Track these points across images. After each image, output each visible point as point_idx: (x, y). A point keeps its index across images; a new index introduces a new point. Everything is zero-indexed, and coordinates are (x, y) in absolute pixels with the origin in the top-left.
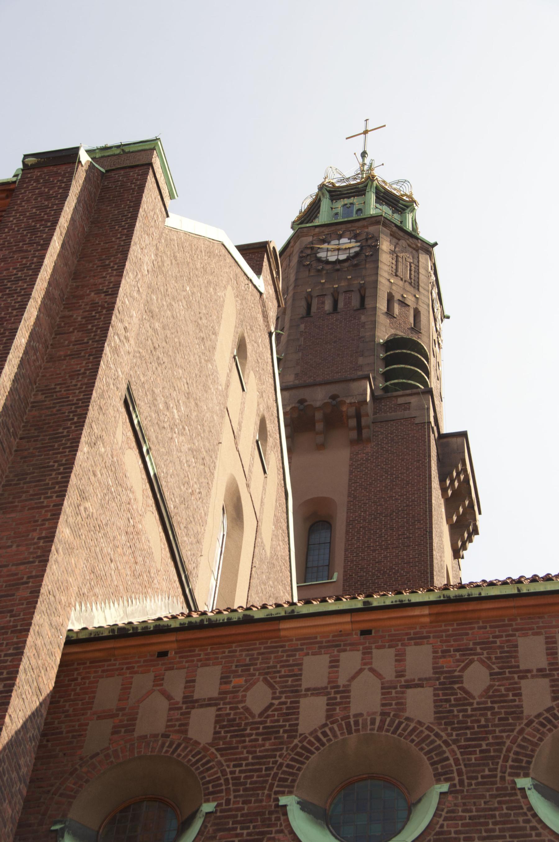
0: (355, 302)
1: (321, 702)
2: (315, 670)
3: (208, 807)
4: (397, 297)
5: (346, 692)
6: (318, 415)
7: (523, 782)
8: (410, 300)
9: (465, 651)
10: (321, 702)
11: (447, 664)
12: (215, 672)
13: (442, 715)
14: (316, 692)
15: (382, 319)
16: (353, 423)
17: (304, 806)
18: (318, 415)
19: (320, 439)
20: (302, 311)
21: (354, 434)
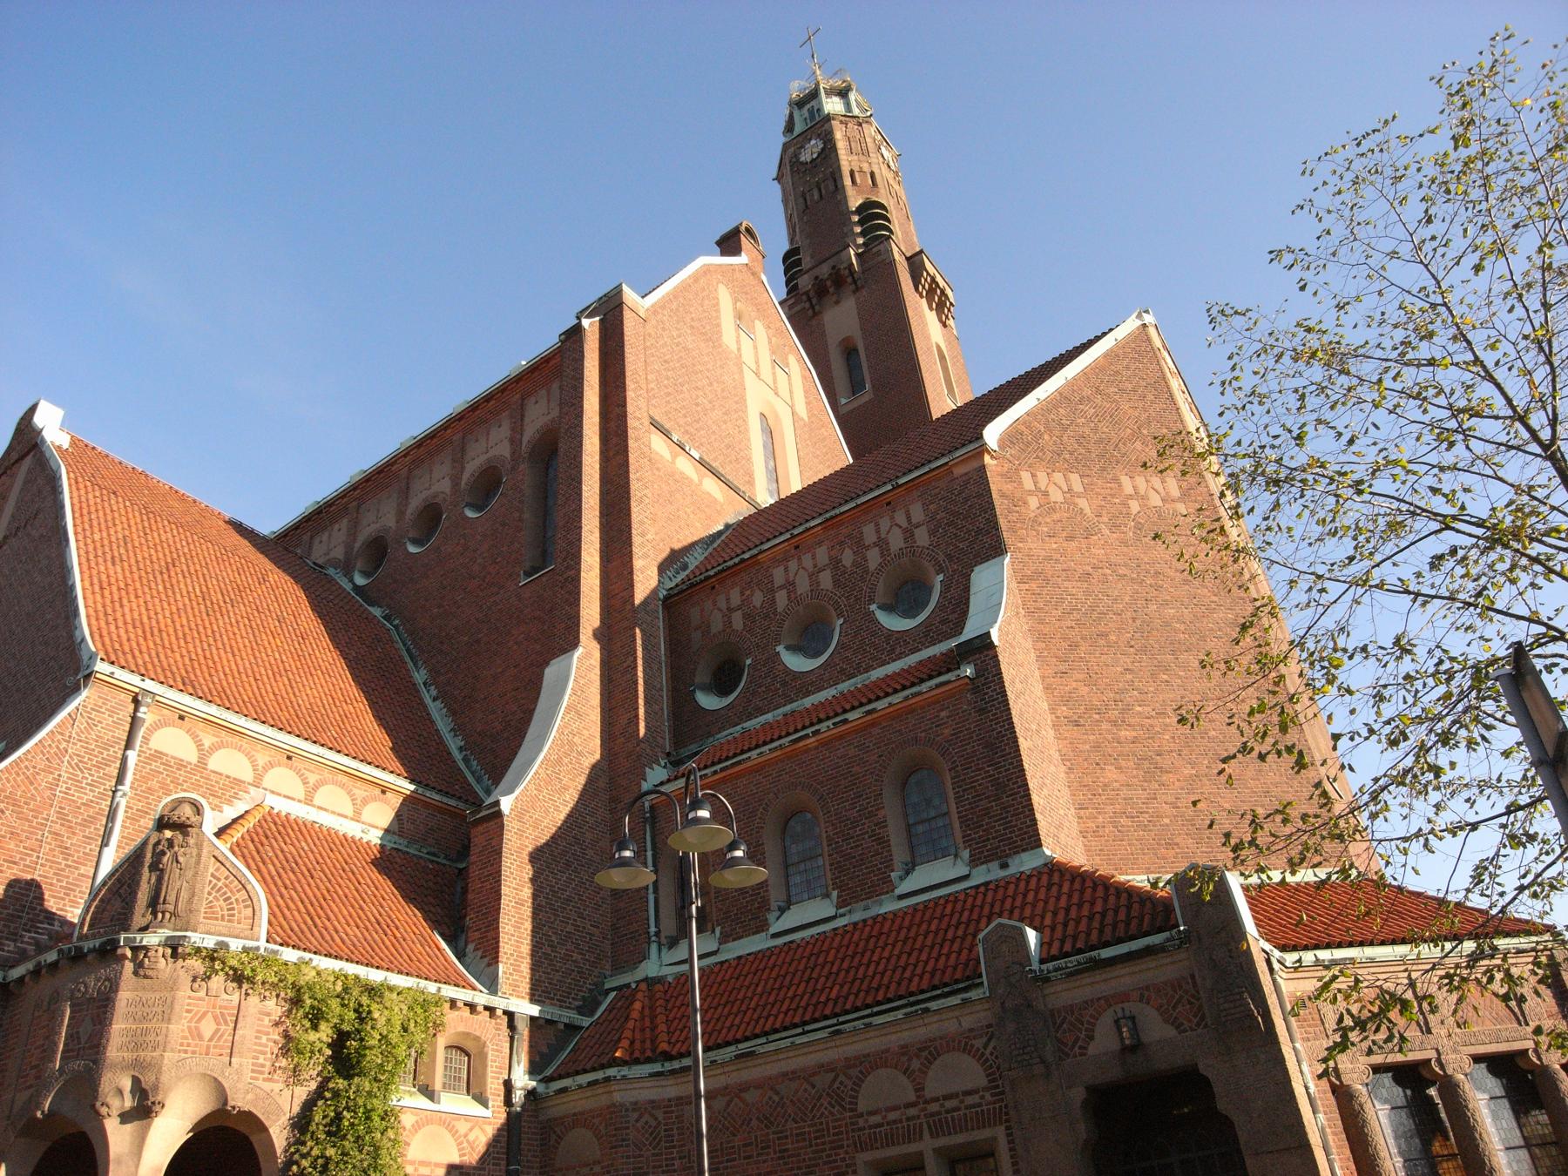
0: (832, 188)
1: (784, 592)
2: (778, 575)
3: (748, 662)
4: (856, 169)
5: (793, 584)
6: (829, 283)
7: (873, 607)
8: (866, 167)
9: (841, 543)
10: (784, 592)
12: (737, 589)
14: (781, 587)
15: (850, 190)
16: (849, 280)
17: (788, 648)
18: (829, 283)
19: (834, 298)
20: (802, 207)
21: (853, 287)
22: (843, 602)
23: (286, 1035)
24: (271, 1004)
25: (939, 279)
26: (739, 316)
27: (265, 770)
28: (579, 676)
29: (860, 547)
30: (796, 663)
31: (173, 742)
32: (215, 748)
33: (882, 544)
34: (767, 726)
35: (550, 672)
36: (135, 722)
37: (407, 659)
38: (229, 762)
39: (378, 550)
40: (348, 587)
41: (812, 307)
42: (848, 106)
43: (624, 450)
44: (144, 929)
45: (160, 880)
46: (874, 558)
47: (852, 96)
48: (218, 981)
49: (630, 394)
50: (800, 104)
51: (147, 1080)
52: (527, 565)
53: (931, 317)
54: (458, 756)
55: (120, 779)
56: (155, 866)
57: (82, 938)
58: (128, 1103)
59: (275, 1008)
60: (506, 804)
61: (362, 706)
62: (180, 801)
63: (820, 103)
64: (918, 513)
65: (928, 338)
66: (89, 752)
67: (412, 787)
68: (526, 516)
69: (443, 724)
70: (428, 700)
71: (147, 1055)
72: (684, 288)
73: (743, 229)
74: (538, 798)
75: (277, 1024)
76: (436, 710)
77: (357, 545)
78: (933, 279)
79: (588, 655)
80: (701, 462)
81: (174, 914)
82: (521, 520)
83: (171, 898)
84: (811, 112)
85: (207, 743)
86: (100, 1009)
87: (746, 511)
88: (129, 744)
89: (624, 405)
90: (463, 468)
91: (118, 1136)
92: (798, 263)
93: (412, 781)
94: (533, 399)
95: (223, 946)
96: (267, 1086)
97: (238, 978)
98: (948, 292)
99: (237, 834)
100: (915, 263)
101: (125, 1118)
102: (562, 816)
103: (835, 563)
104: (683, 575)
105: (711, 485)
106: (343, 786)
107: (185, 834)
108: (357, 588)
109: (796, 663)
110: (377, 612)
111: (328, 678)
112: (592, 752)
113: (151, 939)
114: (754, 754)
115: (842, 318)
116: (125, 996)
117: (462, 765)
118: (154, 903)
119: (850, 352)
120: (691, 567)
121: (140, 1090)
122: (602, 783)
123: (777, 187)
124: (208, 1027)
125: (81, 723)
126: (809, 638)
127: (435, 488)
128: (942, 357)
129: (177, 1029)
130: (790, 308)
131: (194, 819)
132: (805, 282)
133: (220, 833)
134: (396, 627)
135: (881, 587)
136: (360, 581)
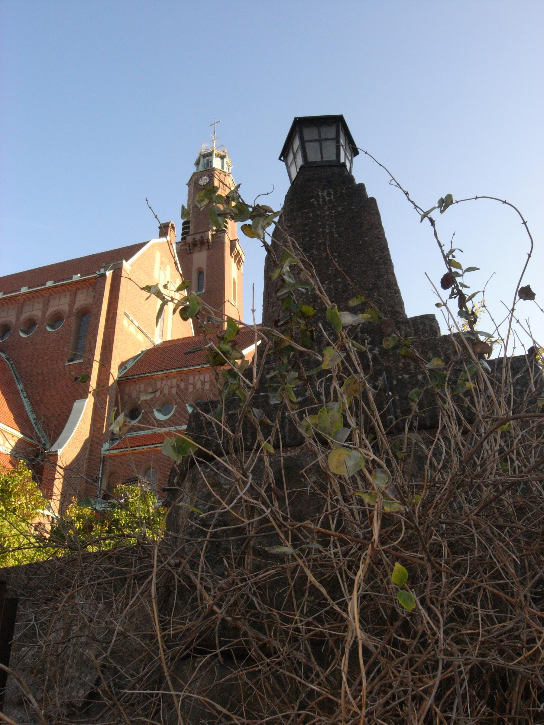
5: (163, 389)
6: (198, 243)
7: (187, 405)
11: (179, 383)
13: (177, 393)
17: (157, 410)
18: (198, 243)
22: (178, 400)
25: (241, 252)
26: (162, 263)
28: (86, 407)
29: (187, 384)
30: (159, 416)
33: (194, 384)
34: (145, 436)
35: (77, 404)
37: (15, 378)
41: (190, 250)
42: (223, 163)
43: (114, 328)
46: (191, 388)
47: (225, 160)
49: (119, 306)
50: (204, 156)
52: (69, 357)
53: (234, 266)
54: (33, 422)
60: (60, 452)
63: (212, 159)
64: (207, 378)
65: (230, 276)
67: (22, 436)
68: (71, 338)
69: (28, 408)
70: (23, 397)
72: (145, 254)
73: (170, 225)
74: (68, 449)
76: (26, 402)
78: (238, 252)
79: (90, 401)
80: (138, 327)
82: (69, 339)
84: (208, 161)
87: (150, 346)
89: (116, 310)
90: (47, 309)
92: (188, 228)
93: (22, 433)
94: (80, 292)
98: (243, 257)
100: (233, 244)
102: (75, 456)
103: (178, 386)
104: (125, 371)
105: (140, 337)
109: (159, 416)
110: (3, 355)
112: (86, 434)
114: (141, 448)
115: (200, 258)
117: (34, 425)
119: (200, 273)
120: (128, 368)
122: (88, 446)
123: (187, 188)
126: (164, 408)
127: (35, 313)
128: (234, 283)
130: (181, 246)
132: (189, 239)
134: (11, 364)
135: (191, 399)
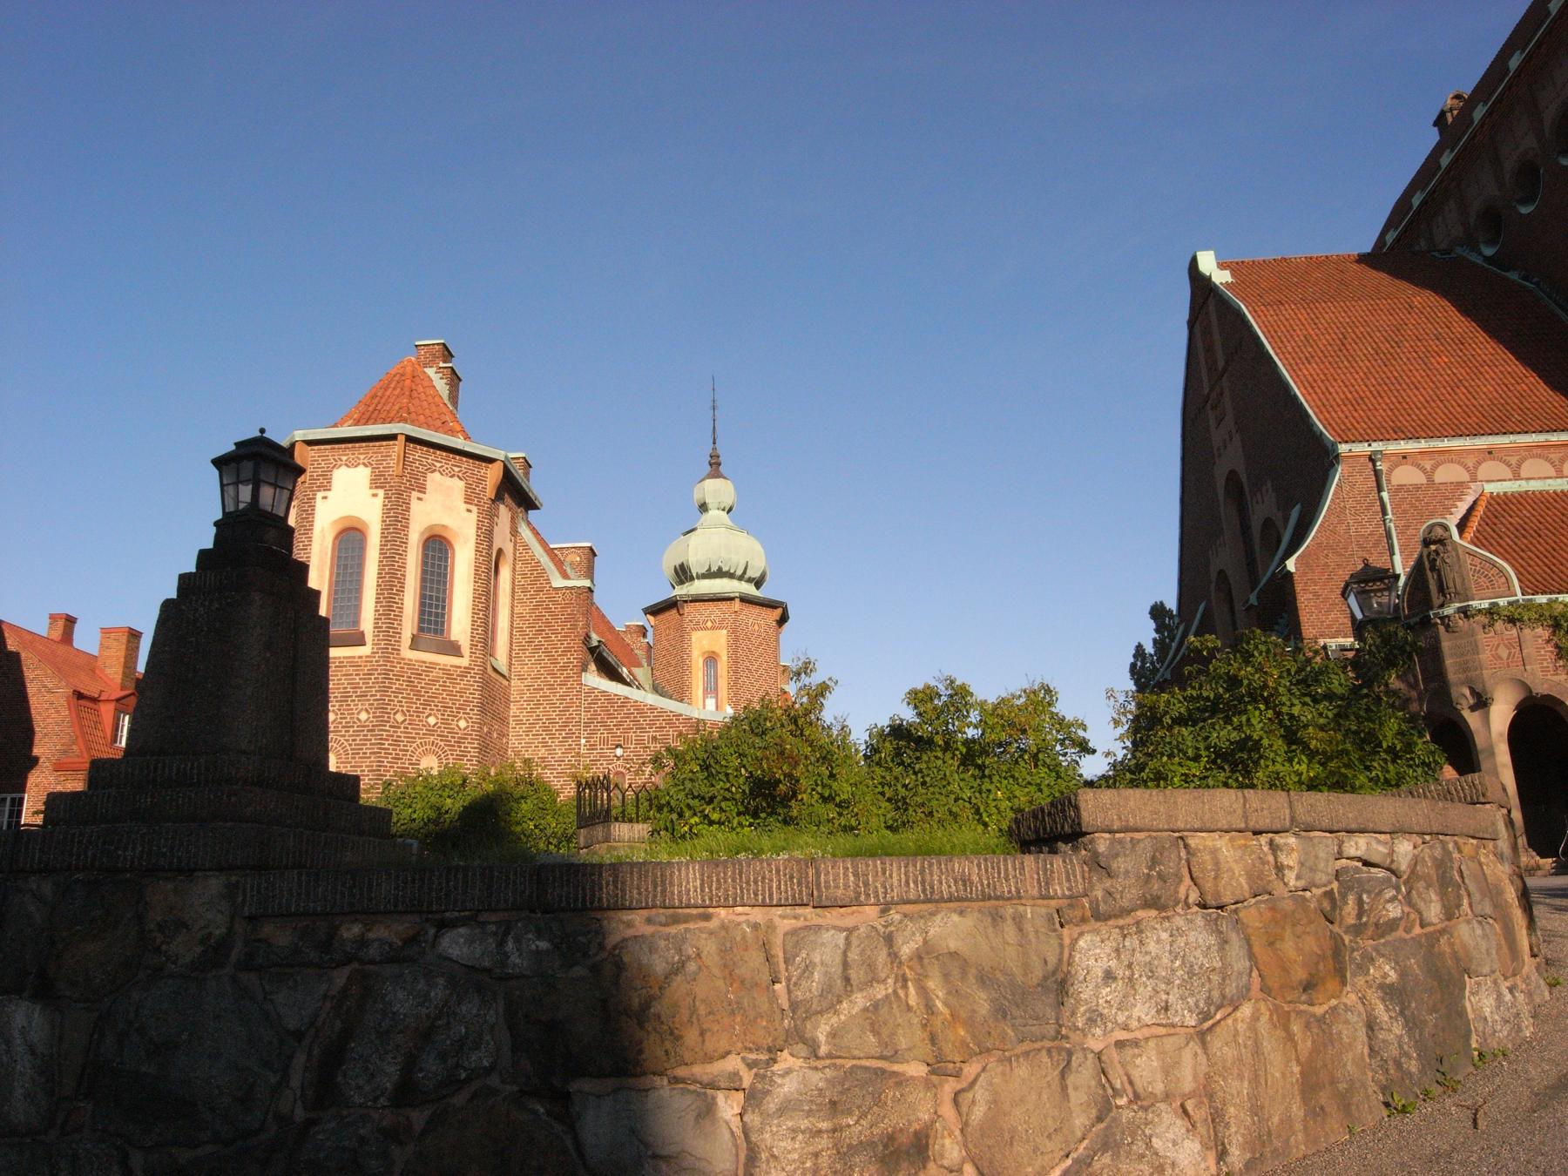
23: (1557, 646)
24: (1539, 630)
27: (1476, 468)
31: (1406, 475)
32: (1434, 468)
36: (1377, 474)
38: (1447, 474)
39: (1494, 220)
40: (1479, 261)
44: (1442, 606)
45: (1439, 575)
48: (1499, 625)
51: (1478, 688)
55: (1384, 512)
56: (1433, 568)
57: (1406, 617)
58: (1472, 702)
59: (1543, 632)
61: (1533, 379)
62: (1433, 526)
66: (1359, 502)
71: (1473, 674)
75: (1548, 641)
77: (1472, 221)
81: (1456, 593)
83: (1451, 585)
85: (1428, 467)
86: (1433, 656)
88: (1380, 489)
91: (1473, 719)
95: (1496, 604)
96: (1555, 678)
97: (1512, 620)
99: (1474, 523)
101: (1473, 708)
106: (1539, 456)
107: (1444, 545)
108: (1486, 259)
110: (1513, 276)
111: (1498, 370)
113: (1449, 610)
116: (1446, 644)
118: (1442, 589)
121: (1473, 692)
124: (1503, 652)
125: (1346, 487)
129: (1485, 656)
131: (1446, 535)
133: (1462, 526)
134: (1537, 284)
136: (1489, 251)
